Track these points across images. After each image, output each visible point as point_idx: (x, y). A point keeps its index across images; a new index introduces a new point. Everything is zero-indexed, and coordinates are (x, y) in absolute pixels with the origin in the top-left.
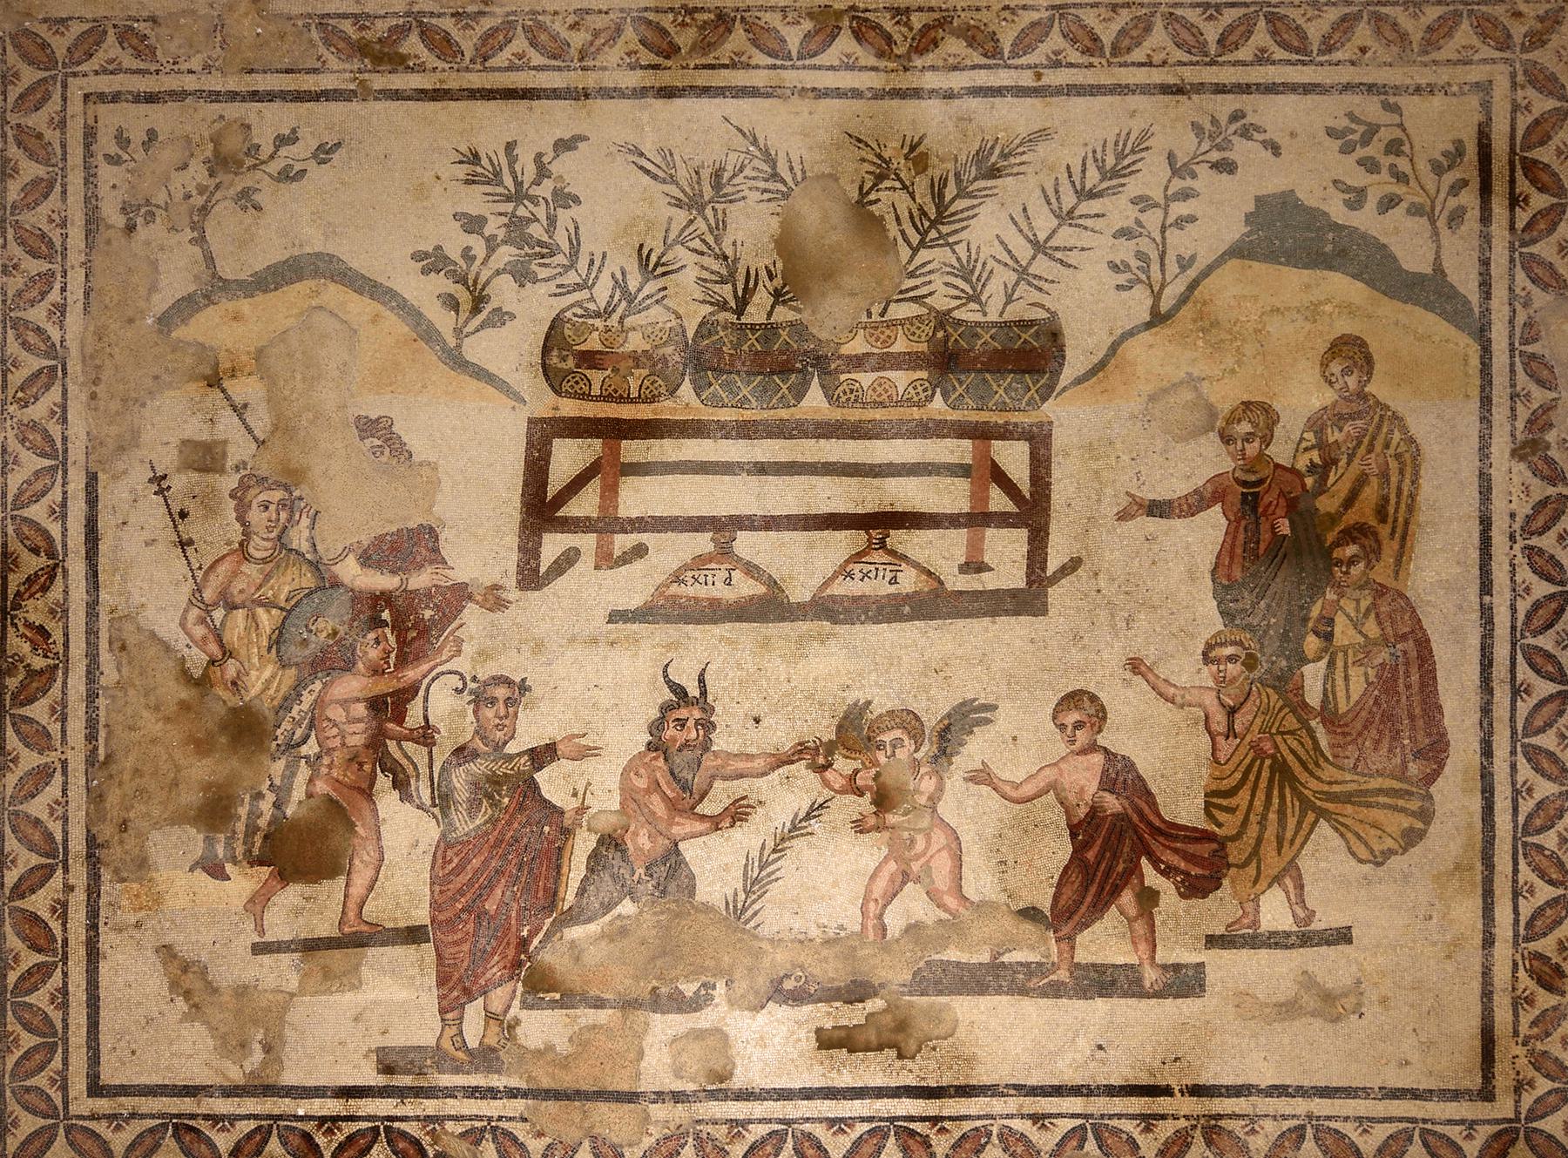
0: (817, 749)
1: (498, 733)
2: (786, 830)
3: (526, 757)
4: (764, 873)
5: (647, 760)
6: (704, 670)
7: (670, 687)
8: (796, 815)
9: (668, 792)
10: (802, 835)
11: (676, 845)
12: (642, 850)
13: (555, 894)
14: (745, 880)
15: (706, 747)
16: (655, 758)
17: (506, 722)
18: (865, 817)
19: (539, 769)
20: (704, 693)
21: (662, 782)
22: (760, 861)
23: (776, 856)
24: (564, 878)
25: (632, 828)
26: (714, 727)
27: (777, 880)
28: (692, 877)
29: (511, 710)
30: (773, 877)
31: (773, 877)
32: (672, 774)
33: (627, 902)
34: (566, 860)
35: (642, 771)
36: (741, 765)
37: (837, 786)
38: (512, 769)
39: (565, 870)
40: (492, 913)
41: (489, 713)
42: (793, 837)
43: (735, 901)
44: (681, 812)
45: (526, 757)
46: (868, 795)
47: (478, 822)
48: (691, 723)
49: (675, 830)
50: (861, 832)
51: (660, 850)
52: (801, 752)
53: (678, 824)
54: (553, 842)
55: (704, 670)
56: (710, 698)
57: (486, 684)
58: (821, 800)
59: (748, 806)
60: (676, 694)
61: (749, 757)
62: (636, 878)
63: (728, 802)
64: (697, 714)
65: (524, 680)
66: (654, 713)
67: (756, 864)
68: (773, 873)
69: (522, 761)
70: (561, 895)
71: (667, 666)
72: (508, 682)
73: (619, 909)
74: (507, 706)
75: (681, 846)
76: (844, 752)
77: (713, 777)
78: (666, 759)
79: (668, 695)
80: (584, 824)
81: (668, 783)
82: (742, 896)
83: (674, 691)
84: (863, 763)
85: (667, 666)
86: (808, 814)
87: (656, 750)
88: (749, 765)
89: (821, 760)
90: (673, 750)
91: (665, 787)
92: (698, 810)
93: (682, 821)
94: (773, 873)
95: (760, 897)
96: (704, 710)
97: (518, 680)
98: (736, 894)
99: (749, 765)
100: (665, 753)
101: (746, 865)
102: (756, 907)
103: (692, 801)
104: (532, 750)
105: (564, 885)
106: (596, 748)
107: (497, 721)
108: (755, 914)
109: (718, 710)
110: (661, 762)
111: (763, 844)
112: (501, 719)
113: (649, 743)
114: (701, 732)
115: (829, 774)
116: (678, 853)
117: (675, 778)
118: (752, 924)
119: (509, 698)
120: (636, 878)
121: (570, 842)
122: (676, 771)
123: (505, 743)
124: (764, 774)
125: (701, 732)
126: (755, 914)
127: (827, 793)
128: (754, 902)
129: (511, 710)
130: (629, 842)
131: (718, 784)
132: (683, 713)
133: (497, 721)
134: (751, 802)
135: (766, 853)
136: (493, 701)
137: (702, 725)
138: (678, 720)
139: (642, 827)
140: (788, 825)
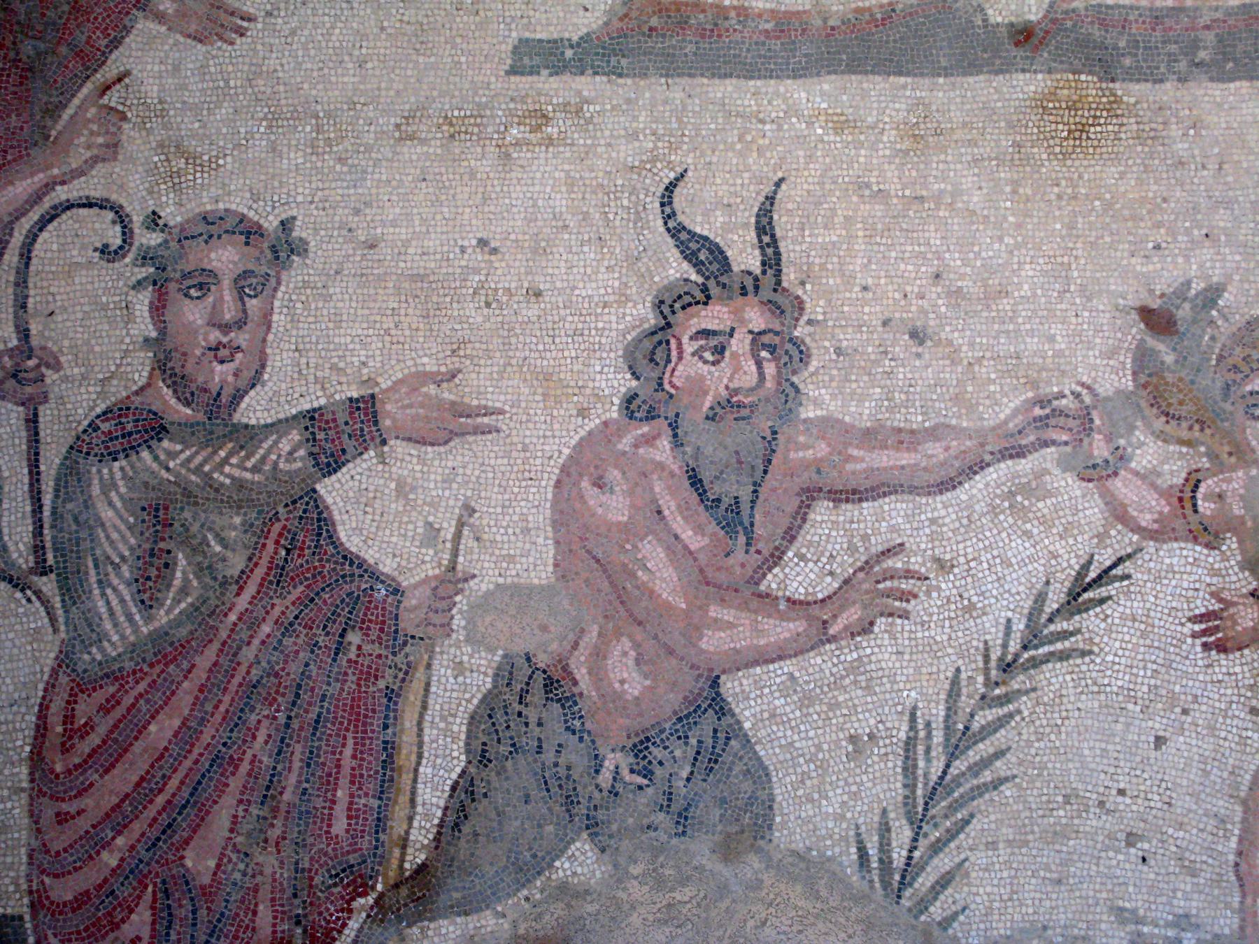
0: (1085, 418)
1: (218, 368)
2: (1014, 646)
3: (295, 436)
4: (959, 766)
5: (625, 444)
6: (771, 199)
7: (682, 247)
8: (1041, 598)
9: (687, 535)
10: (1063, 656)
11: (715, 683)
12: (618, 696)
13: (381, 823)
14: (911, 787)
15: (789, 395)
16: (649, 440)
17: (242, 338)
18: (1228, 604)
19: (331, 464)
20: (773, 262)
21: (669, 506)
22: (948, 728)
23: (990, 715)
24: (406, 779)
25: (592, 636)
26: (804, 357)
27: (997, 784)
28: (760, 774)
29: (252, 304)
30: (987, 776)
31: (987, 776)
32: (695, 481)
33: (582, 848)
34: (409, 721)
35: (614, 474)
36: (883, 459)
37: (1146, 520)
38: (255, 469)
39: (405, 757)
40: (206, 880)
41: (192, 313)
42: (1035, 663)
43: (885, 847)
44: (726, 592)
45: (295, 436)
46: (1231, 543)
47: (162, 618)
48: (740, 344)
49: (712, 642)
50: (1222, 648)
51: (672, 701)
52: (1042, 422)
53: (717, 624)
54: (372, 675)
55: (771, 199)
56: (790, 277)
57: (185, 237)
58: (1105, 558)
59: (908, 574)
60: (698, 265)
61: (907, 438)
62: (605, 778)
63: (846, 565)
64: (756, 318)
65: (286, 225)
66: (643, 314)
67: (938, 737)
68: (986, 763)
69: (285, 446)
70: (398, 828)
71: (670, 188)
72: (249, 232)
73: (563, 867)
74: (241, 295)
75: (729, 686)
76: (1159, 423)
77: (809, 495)
78: (677, 442)
79: (676, 269)
80: (458, 622)
81: (683, 509)
82: (902, 834)
83: (690, 256)
84: (1213, 456)
85: (670, 188)
86: (1073, 596)
87: (651, 416)
88: (906, 459)
89: (1099, 449)
90: (693, 421)
91: (678, 524)
92: (771, 582)
93: (727, 615)
94: (986, 763)
95: (952, 835)
96: (775, 308)
97: (271, 223)
98: (885, 829)
99: (906, 459)
100: (674, 426)
101: (910, 744)
102: (943, 862)
103: (755, 559)
104: (312, 416)
105: (404, 799)
106: (489, 412)
107: (215, 336)
108: (944, 882)
109: (815, 308)
110: (663, 450)
111: (955, 682)
112: (225, 328)
113: (630, 399)
114: (770, 369)
115: (1123, 487)
116: (719, 706)
117: (702, 495)
118: (937, 911)
119: (247, 274)
120: (605, 778)
121: (420, 674)
122: (706, 475)
123: (238, 397)
124: (948, 485)
125: (770, 369)
126: (944, 882)
127: (1123, 540)
128: (937, 848)
129: (252, 304)
130: (581, 673)
131: (822, 512)
132: (714, 316)
133: (215, 336)
134: (915, 563)
135: (966, 703)
136: (204, 282)
137: (772, 349)
138: (705, 333)
139: (618, 634)
140: (1019, 626)
